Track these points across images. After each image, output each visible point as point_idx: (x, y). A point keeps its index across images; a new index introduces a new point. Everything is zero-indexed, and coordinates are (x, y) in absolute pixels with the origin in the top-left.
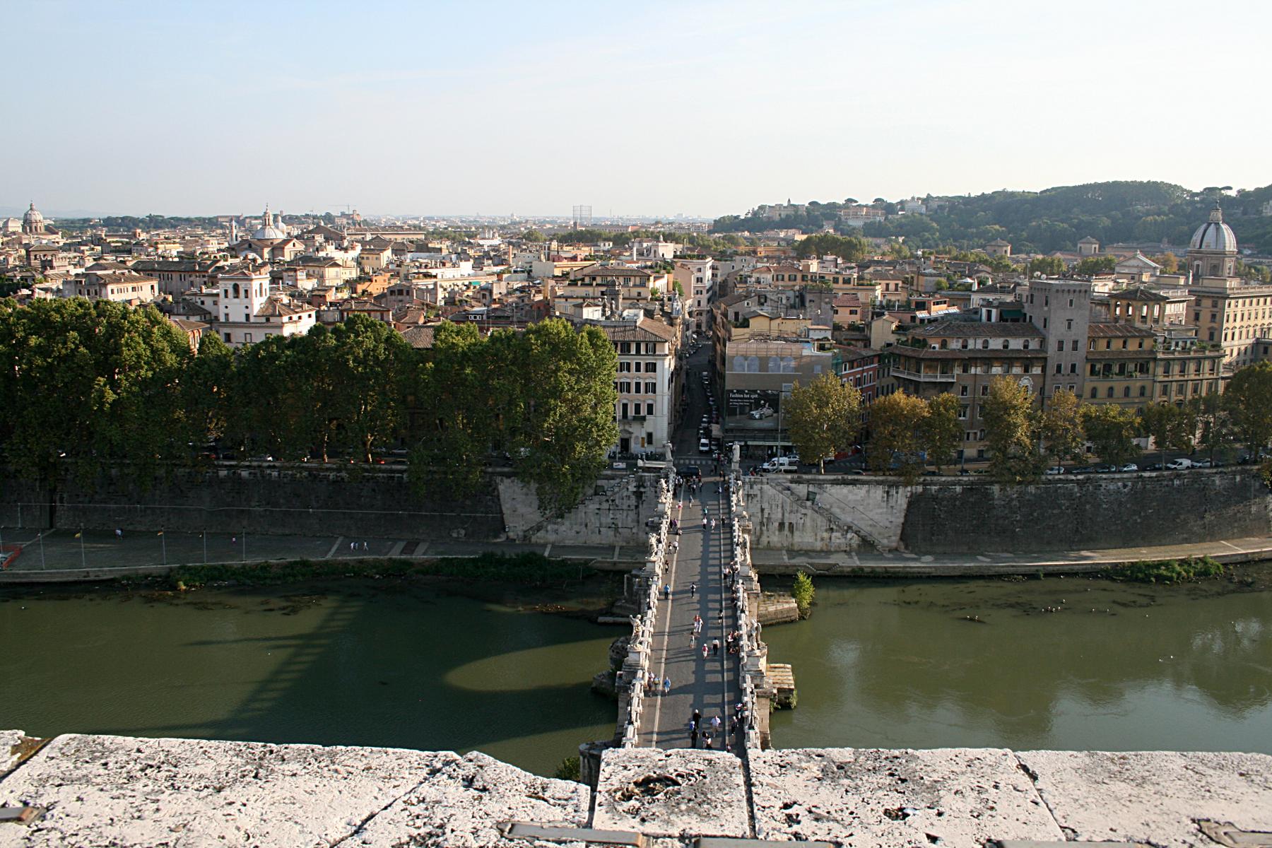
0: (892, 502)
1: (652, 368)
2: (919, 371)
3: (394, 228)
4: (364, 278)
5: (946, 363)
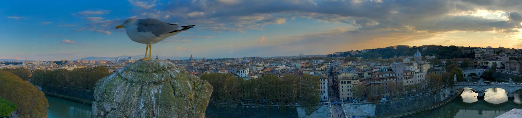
1: (324, 84)
3: (268, 59)
4: (265, 68)
5: (379, 80)
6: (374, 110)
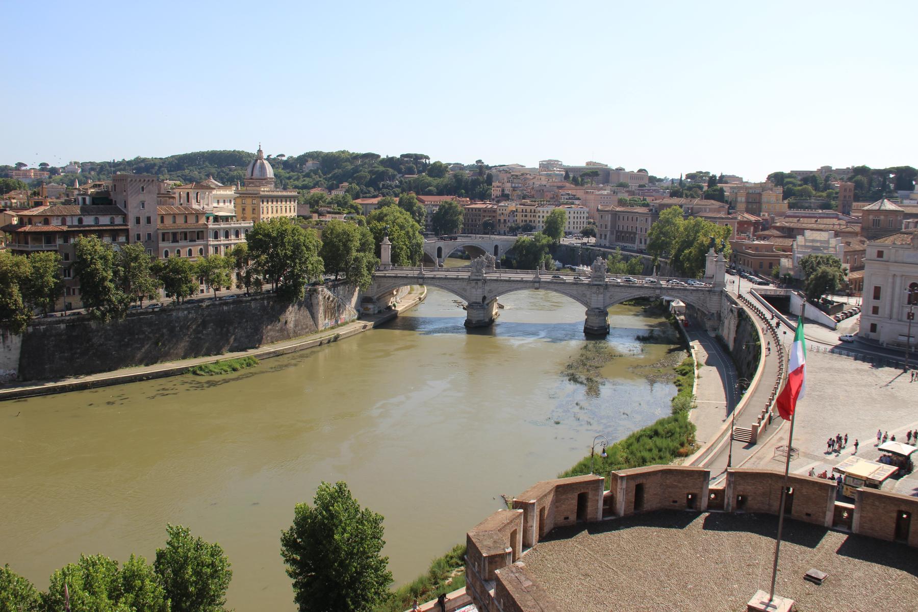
0: (8, 342)
2: (27, 243)
6: (15, 355)
